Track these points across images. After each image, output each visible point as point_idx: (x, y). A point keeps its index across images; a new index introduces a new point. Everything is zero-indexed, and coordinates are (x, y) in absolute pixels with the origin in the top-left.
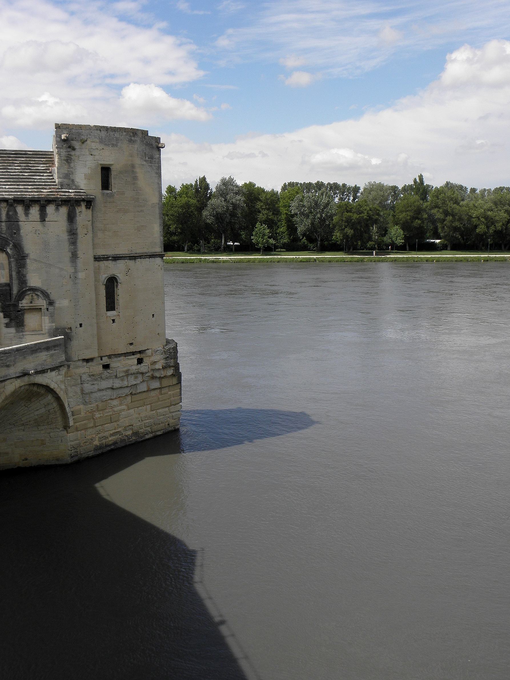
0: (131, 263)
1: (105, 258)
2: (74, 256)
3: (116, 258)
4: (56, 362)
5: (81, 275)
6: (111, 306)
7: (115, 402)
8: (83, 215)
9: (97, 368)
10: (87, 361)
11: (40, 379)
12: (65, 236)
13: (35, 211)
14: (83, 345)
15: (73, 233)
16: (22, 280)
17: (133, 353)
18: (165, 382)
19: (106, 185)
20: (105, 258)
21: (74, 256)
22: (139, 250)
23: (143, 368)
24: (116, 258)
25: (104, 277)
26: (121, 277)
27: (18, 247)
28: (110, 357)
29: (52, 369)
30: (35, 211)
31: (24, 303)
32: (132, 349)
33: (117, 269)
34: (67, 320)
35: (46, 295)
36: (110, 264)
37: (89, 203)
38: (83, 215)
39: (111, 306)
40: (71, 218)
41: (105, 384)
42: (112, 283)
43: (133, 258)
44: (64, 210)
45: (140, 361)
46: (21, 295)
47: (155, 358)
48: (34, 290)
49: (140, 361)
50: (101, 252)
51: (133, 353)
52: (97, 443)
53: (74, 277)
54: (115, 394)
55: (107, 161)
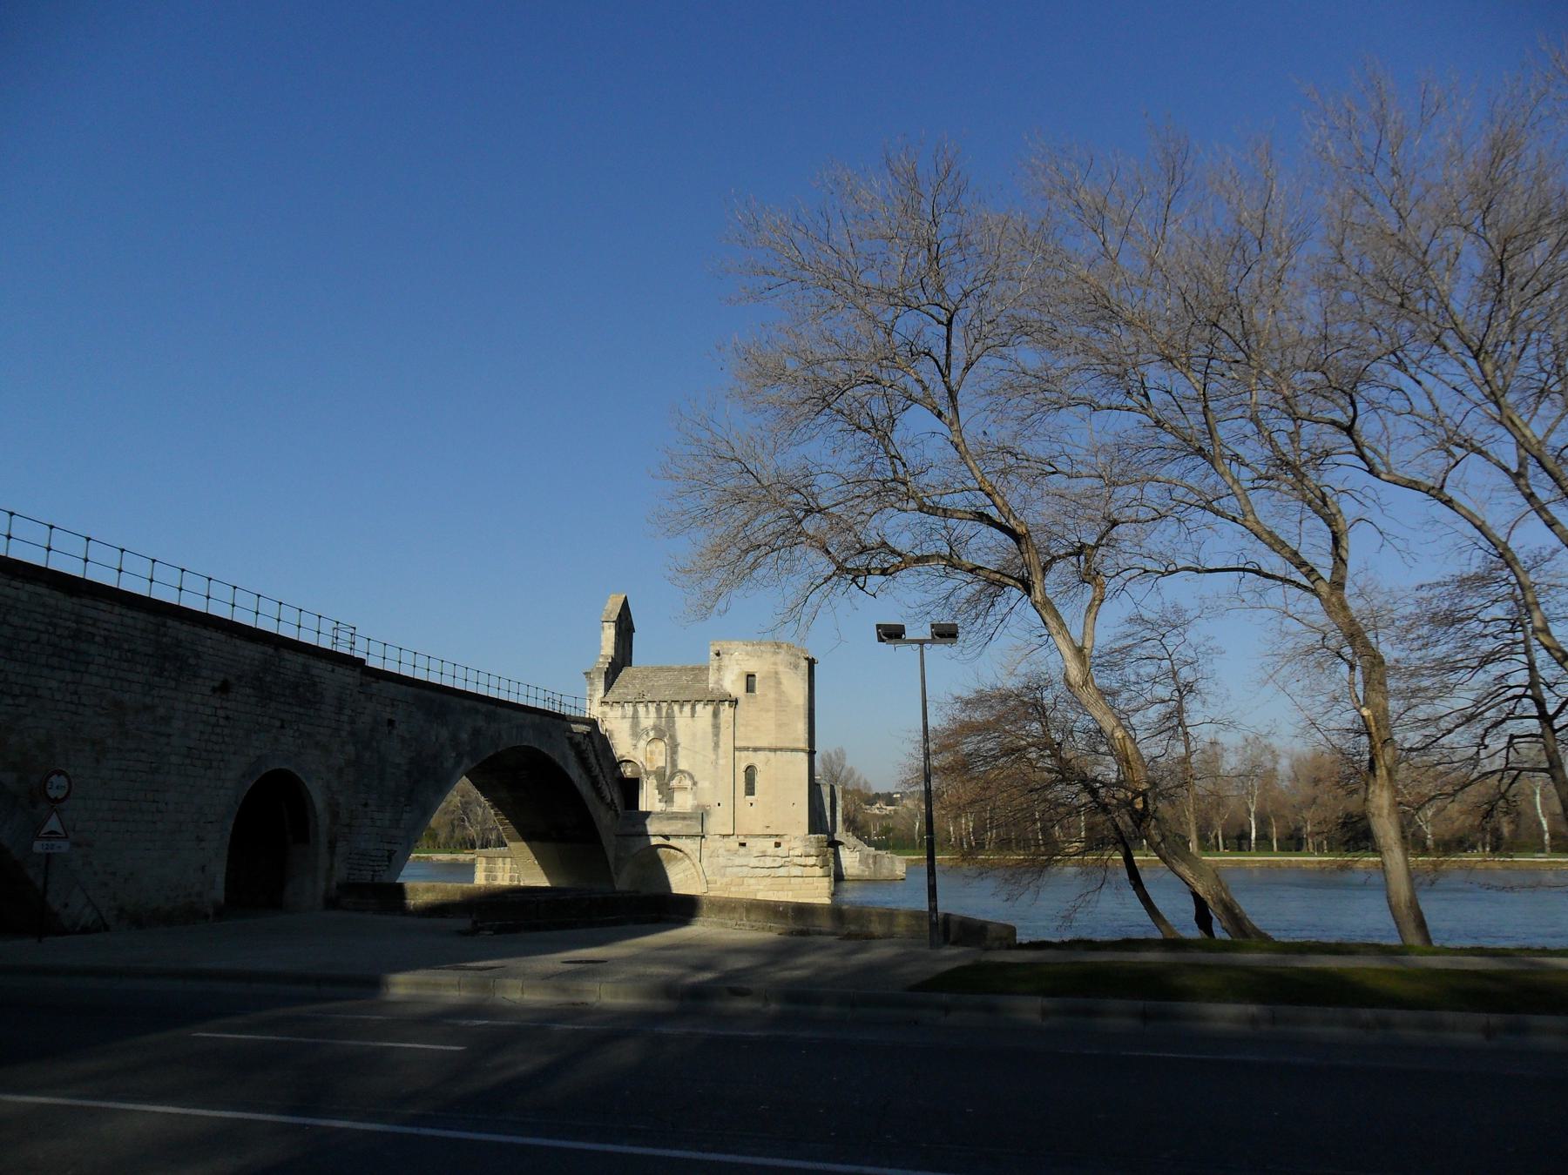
1: (747, 749)
2: (716, 745)
3: (756, 750)
5: (721, 762)
6: (750, 790)
7: (752, 881)
8: (726, 710)
9: (733, 843)
12: (710, 729)
13: (687, 708)
15: (716, 727)
16: (674, 763)
17: (771, 836)
19: (750, 688)
20: (747, 749)
21: (716, 745)
22: (780, 745)
23: (780, 851)
24: (756, 750)
25: (743, 766)
26: (759, 767)
27: (673, 738)
30: (687, 708)
31: (674, 783)
32: (769, 831)
33: (758, 760)
34: (707, 799)
35: (692, 777)
36: (751, 753)
37: (734, 702)
39: (750, 790)
40: (716, 714)
41: (738, 861)
42: (750, 772)
44: (710, 708)
45: (778, 845)
46: (672, 777)
47: (793, 844)
48: (682, 772)
49: (778, 845)
51: (771, 836)
53: (715, 763)
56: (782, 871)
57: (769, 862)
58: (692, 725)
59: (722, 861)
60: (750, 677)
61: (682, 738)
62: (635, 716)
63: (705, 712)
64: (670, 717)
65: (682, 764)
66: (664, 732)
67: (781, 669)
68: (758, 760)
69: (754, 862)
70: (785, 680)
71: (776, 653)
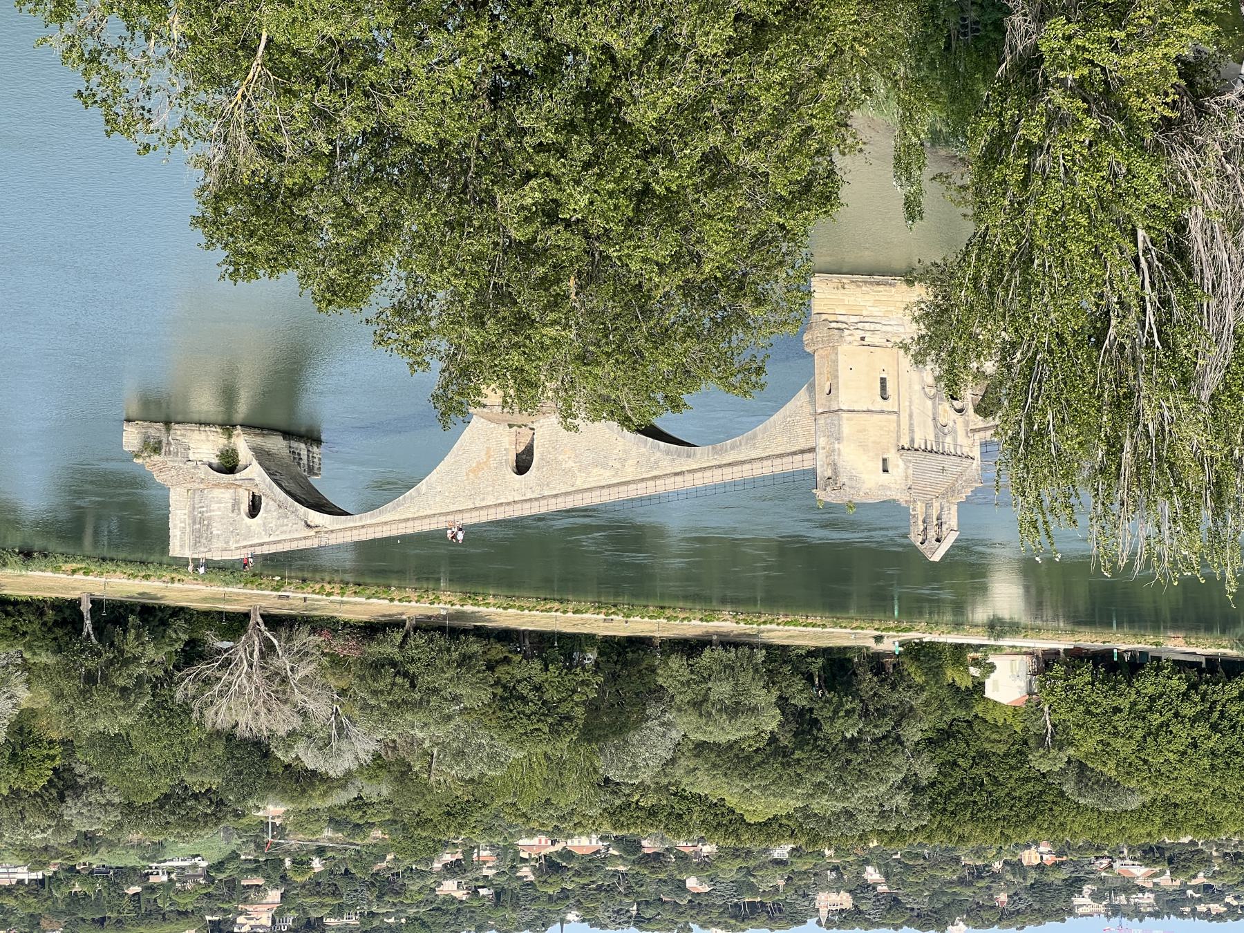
2: (911, 416)
6: (883, 381)
15: (912, 431)
21: (911, 416)
22: (864, 415)
25: (890, 401)
27: (935, 426)
34: (915, 376)
39: (883, 381)
40: (912, 441)
41: (889, 329)
49: (863, 339)
50: (894, 417)
55: (886, 475)
57: (867, 326)
58: (924, 435)
62: (956, 445)
64: (938, 442)
65: (929, 403)
66: (941, 429)
68: (880, 404)
69: (878, 327)
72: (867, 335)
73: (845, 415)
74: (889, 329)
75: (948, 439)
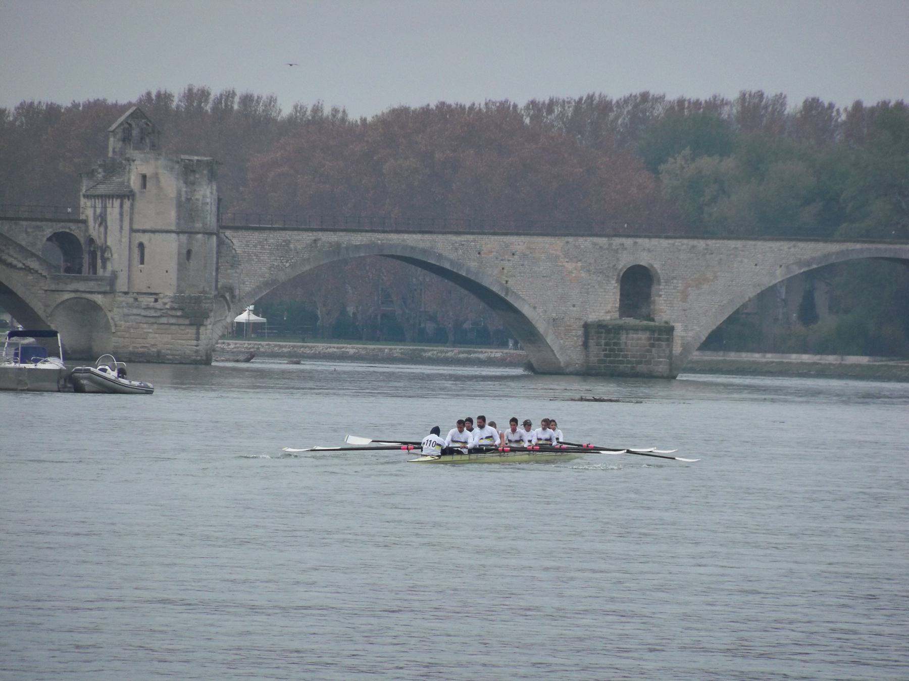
0: (152, 235)
1: (138, 231)
2: (121, 228)
3: (144, 231)
4: (103, 289)
5: (123, 240)
6: (142, 262)
7: (145, 326)
10: (126, 293)
11: (88, 296)
12: (118, 216)
14: (121, 284)
15: (121, 214)
17: (151, 294)
18: (181, 321)
19: (144, 185)
20: (138, 231)
21: (121, 228)
24: (144, 231)
25: (137, 242)
26: (146, 243)
28: (138, 293)
29: (99, 293)
32: (149, 291)
33: (144, 238)
37: (131, 195)
38: (127, 204)
40: (121, 206)
41: (135, 311)
42: (141, 246)
43: (154, 232)
44: (119, 201)
45: (156, 301)
49: (156, 301)
50: (136, 227)
51: (151, 294)
52: (131, 349)
53: (120, 241)
54: (144, 320)
56: (164, 320)
57: (152, 313)
59: (126, 310)
60: (144, 177)
61: (109, 223)
63: (117, 203)
64: (105, 208)
65: (109, 243)
66: (102, 220)
67: (161, 171)
69: (143, 313)
70: (163, 180)
71: (157, 159)
72: (152, 304)
73: (173, 228)
74: (135, 311)
75: (98, 211)
